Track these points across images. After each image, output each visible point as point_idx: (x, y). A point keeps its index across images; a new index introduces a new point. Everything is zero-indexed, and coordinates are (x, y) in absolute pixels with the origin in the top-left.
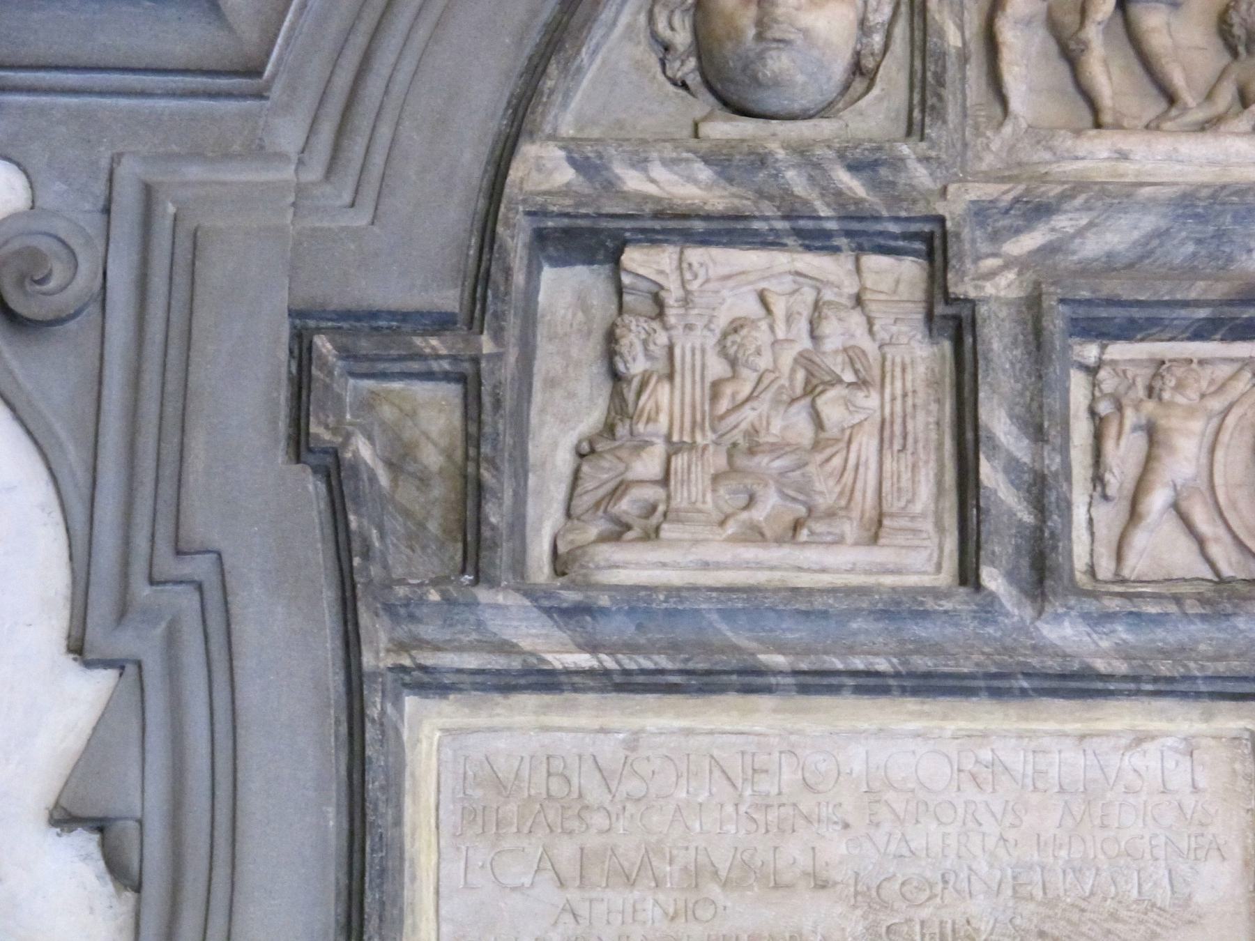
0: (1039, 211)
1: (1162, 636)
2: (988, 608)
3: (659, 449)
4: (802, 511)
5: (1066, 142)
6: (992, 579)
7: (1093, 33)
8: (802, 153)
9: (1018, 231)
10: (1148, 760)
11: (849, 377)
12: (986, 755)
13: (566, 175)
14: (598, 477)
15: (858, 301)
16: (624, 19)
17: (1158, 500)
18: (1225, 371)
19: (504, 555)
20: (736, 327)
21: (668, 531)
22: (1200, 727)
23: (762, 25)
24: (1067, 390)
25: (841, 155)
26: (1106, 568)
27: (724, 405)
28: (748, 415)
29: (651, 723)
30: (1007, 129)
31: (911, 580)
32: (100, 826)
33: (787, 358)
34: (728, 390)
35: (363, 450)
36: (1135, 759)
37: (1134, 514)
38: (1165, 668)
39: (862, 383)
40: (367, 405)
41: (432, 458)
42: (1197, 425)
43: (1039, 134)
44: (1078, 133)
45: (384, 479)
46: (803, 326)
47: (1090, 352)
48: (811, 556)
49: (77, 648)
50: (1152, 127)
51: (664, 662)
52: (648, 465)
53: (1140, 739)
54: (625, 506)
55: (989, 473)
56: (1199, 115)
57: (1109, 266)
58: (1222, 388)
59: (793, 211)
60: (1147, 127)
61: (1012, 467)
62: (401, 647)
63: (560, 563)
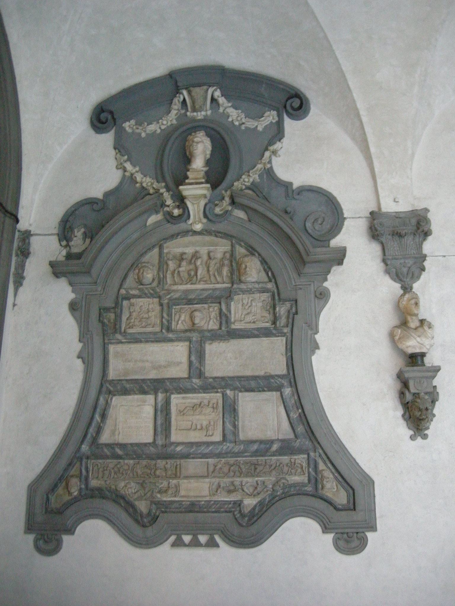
0: (169, 294)
1: (180, 336)
2: (163, 333)
3: (133, 319)
4: (146, 324)
5: (172, 286)
6: (164, 331)
7: (176, 275)
8: (147, 288)
9: (167, 296)
10: (178, 348)
11: (152, 311)
12: (163, 348)
13: (125, 292)
14: (128, 322)
15: (153, 303)
16: (131, 276)
17: (180, 322)
18: (187, 308)
19: (118, 331)
20: (141, 306)
21: (134, 327)
22: (183, 344)
23: (143, 276)
24: (172, 311)
25: (151, 289)
26: (175, 329)
27: (140, 314)
28: (142, 315)
29: (132, 346)
30: (167, 285)
31: (157, 331)
32: (82, 358)
33: (146, 309)
34: (140, 313)
35: (105, 321)
36: (176, 348)
37: (178, 324)
38: (179, 339)
39: (153, 311)
40: (106, 316)
41: (112, 321)
42: (184, 314)
43: (170, 285)
44: (174, 285)
45: (108, 323)
46: (147, 306)
47: (174, 307)
48: (147, 329)
49: (80, 341)
50: (181, 284)
51: (133, 340)
52: (132, 321)
53: (178, 346)
54: (131, 324)
55: (164, 320)
56: (185, 283)
57: (176, 299)
58: (187, 310)
59: (146, 294)
60: (180, 284)
61: (166, 319)
62: (109, 340)
63: (125, 330)
